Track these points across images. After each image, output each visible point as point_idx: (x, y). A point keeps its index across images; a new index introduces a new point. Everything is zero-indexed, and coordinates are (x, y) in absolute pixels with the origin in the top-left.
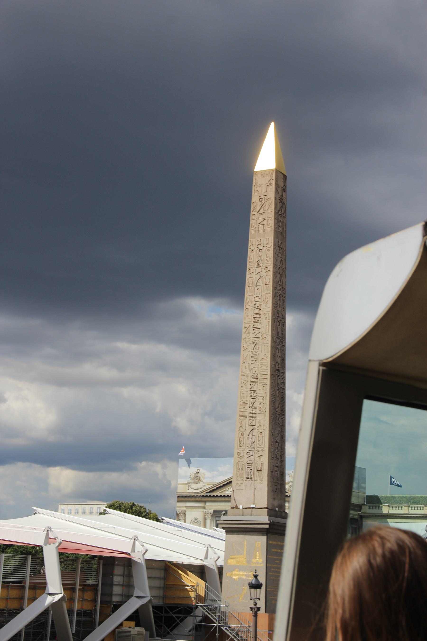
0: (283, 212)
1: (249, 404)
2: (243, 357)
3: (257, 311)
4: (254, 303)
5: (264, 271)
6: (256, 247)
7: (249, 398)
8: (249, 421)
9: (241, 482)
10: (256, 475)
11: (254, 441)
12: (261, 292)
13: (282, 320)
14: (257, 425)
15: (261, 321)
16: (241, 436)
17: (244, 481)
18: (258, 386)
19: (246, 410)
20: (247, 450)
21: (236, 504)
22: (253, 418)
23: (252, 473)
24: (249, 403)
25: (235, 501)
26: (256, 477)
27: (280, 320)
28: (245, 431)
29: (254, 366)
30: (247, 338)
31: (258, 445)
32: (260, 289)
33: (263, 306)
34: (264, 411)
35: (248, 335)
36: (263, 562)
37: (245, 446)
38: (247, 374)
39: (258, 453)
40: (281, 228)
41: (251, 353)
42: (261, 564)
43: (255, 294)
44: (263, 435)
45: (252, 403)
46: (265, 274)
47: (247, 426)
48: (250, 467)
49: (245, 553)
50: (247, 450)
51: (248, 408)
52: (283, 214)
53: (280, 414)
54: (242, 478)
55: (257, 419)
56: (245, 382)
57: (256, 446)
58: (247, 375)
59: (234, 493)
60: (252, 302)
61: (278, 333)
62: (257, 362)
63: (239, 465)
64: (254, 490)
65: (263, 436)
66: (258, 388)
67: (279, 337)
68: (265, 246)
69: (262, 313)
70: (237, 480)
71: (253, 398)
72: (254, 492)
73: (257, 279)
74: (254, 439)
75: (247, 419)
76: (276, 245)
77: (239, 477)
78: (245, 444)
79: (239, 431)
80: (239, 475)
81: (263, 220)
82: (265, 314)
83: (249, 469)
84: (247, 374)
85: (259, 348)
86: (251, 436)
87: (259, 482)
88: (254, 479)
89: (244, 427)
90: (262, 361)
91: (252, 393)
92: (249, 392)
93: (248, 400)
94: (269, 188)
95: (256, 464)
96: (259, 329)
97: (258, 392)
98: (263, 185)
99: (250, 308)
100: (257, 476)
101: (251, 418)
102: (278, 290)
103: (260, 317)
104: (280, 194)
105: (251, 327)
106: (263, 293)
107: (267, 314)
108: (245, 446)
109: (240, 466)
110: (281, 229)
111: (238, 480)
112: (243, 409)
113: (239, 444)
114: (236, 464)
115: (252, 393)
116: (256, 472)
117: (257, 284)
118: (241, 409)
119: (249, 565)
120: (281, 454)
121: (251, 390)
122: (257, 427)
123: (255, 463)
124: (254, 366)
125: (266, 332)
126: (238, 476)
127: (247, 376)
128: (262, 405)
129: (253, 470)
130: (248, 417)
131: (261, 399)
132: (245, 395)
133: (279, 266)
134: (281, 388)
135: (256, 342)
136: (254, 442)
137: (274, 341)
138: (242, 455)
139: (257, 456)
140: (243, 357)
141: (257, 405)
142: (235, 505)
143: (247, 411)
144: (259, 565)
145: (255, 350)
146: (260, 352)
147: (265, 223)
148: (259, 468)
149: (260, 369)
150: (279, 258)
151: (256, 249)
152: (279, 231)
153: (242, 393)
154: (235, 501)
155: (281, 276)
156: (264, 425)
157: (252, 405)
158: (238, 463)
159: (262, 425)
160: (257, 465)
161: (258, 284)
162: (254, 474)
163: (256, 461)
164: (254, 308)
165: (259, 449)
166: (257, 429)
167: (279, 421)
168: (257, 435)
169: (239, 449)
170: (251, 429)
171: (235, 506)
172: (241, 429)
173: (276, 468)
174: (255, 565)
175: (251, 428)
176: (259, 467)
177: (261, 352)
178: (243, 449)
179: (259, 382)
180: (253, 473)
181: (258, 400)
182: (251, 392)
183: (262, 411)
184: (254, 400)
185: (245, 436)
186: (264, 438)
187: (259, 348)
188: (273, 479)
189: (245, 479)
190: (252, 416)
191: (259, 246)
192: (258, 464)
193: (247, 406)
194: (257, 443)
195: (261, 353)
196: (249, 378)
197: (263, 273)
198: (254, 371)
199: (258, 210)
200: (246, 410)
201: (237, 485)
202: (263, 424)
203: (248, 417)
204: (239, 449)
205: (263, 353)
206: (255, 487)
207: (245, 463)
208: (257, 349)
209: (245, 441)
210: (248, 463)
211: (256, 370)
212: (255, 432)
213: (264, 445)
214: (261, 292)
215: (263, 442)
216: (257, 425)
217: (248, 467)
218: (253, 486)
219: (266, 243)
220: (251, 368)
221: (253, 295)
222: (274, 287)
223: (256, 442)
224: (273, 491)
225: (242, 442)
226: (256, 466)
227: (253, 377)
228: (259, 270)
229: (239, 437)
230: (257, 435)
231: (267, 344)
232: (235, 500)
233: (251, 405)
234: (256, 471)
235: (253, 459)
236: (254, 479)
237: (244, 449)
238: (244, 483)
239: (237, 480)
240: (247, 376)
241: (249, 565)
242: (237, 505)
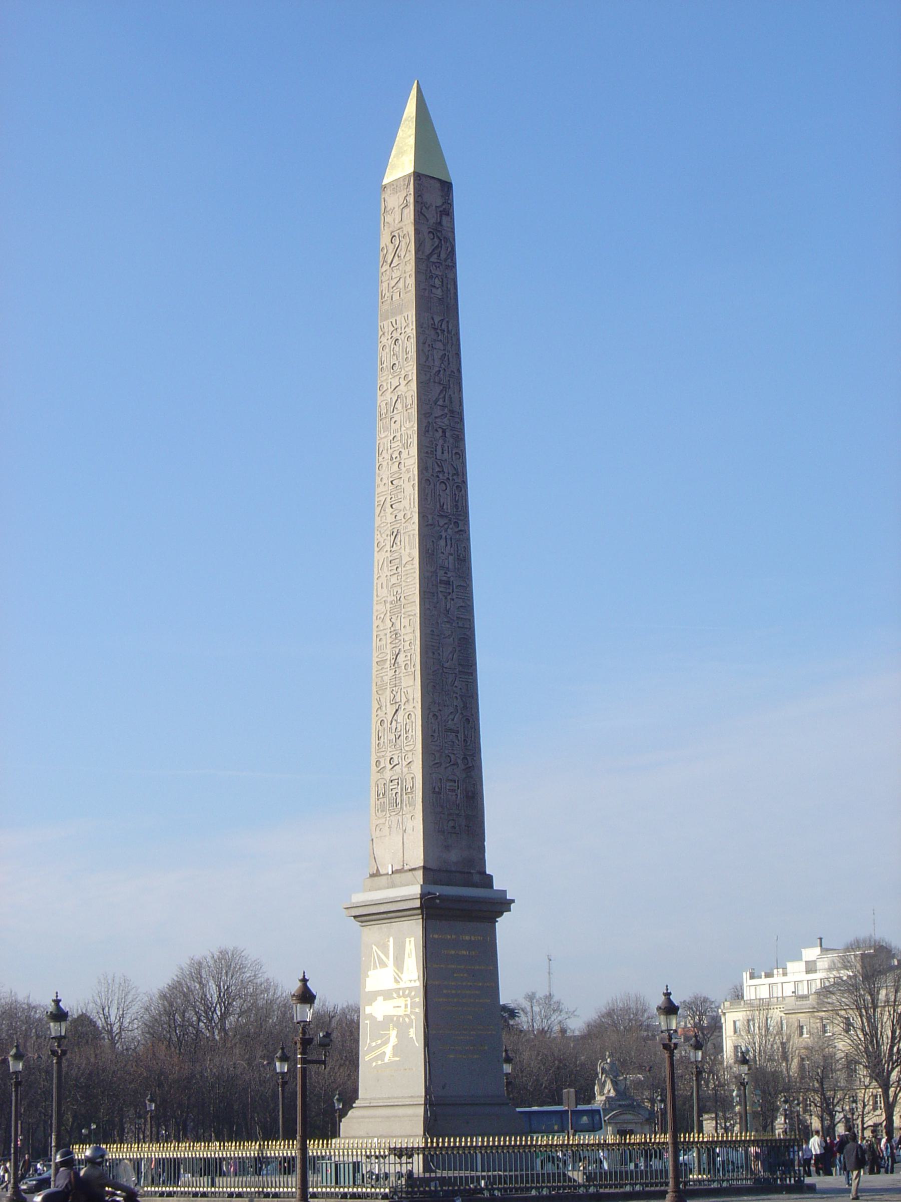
0: (443, 256)
4: (390, 451)
6: (390, 338)
8: (392, 695)
10: (404, 804)
11: (399, 734)
13: (455, 477)
14: (404, 700)
15: (402, 487)
17: (388, 819)
25: (375, 861)
27: (448, 479)
28: (386, 716)
29: (394, 580)
30: (382, 525)
32: (398, 423)
34: (413, 670)
40: (440, 289)
41: (388, 554)
43: (392, 433)
45: (395, 657)
47: (388, 704)
52: (446, 260)
53: (457, 671)
58: (385, 601)
61: (442, 507)
62: (399, 570)
67: (448, 514)
69: (404, 469)
71: (394, 646)
74: (399, 729)
75: (388, 691)
76: (425, 326)
81: (398, 279)
82: (408, 471)
87: (409, 816)
90: (407, 568)
92: (389, 635)
93: (389, 652)
94: (406, 211)
96: (401, 502)
98: (396, 209)
100: (406, 805)
101: (394, 688)
102: (436, 418)
103: (401, 478)
104: (432, 221)
105: (388, 499)
106: (403, 428)
109: (380, 789)
110: (439, 292)
112: (381, 672)
118: (378, 673)
120: (465, 754)
122: (402, 704)
124: (394, 580)
125: (410, 507)
132: (383, 642)
133: (437, 369)
134: (457, 618)
136: (400, 736)
137: (430, 522)
139: (405, 763)
141: (401, 658)
143: (387, 675)
149: (404, 584)
150: (435, 351)
151: (390, 341)
152: (432, 296)
154: (375, 861)
155: (445, 388)
159: (411, 699)
160: (406, 782)
165: (407, 748)
166: (402, 709)
167: (456, 687)
170: (395, 710)
173: (449, 784)
179: (403, 610)
181: (402, 650)
183: (409, 670)
188: (442, 807)
190: (394, 682)
193: (388, 664)
199: (389, 262)
204: (378, 754)
207: (388, 781)
209: (386, 737)
215: (414, 732)
219: (404, 324)
220: (390, 584)
222: (423, 412)
224: (441, 831)
226: (404, 784)
231: (412, 532)
233: (393, 662)
237: (385, 753)
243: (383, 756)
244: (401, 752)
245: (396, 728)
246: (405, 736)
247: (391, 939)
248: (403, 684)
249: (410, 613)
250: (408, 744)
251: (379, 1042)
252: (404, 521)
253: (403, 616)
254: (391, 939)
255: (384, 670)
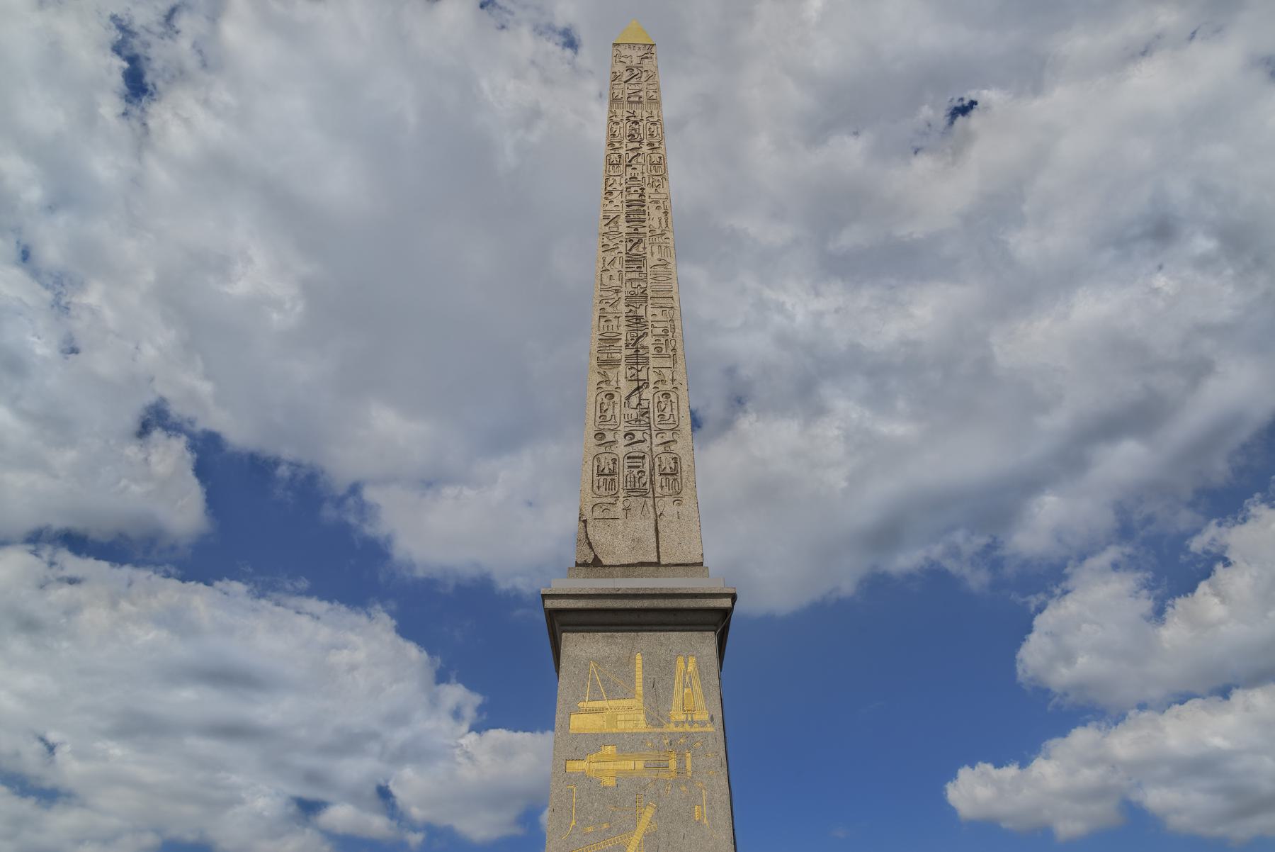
1: (627, 340)
2: (604, 261)
3: (636, 197)
4: (625, 186)
5: (645, 149)
7: (623, 330)
9: (612, 500)
10: (658, 485)
12: (643, 173)
14: (653, 378)
16: (605, 401)
17: (621, 499)
18: (649, 308)
19: (618, 351)
20: (628, 429)
21: (596, 556)
22: (640, 367)
23: (646, 479)
24: (623, 338)
25: (591, 547)
26: (658, 489)
31: (657, 419)
33: (648, 190)
34: (671, 353)
35: (615, 229)
36: (712, 718)
37: (618, 420)
38: (615, 288)
39: (660, 435)
42: (703, 724)
44: (673, 397)
45: (635, 339)
46: (650, 152)
48: (638, 467)
49: (639, 689)
50: (623, 429)
51: (623, 348)
54: (614, 492)
55: (651, 368)
56: (611, 302)
57: (654, 422)
59: (586, 526)
60: (621, 184)
63: (603, 461)
64: (656, 520)
65: (671, 401)
66: (649, 313)
68: (644, 118)
70: (595, 496)
72: (657, 523)
73: (631, 155)
74: (645, 404)
75: (622, 368)
77: (602, 489)
78: (618, 416)
79: (599, 391)
80: (601, 483)
83: (636, 471)
84: (615, 288)
85: (644, 248)
86: (634, 400)
88: (654, 493)
89: (613, 383)
91: (635, 321)
92: (623, 319)
95: (656, 460)
97: (651, 318)
99: (616, 194)
101: (635, 366)
105: (623, 216)
106: (646, 175)
107: (661, 201)
108: (618, 420)
111: (600, 496)
112: (608, 348)
113: (600, 417)
114: (591, 458)
115: (635, 321)
116: (658, 478)
117: (630, 161)
118: (601, 348)
119: (659, 730)
121: (631, 314)
123: (654, 457)
126: (598, 487)
127: (617, 291)
128: (663, 341)
129: (647, 473)
130: (623, 363)
131: (659, 331)
132: (615, 322)
135: (636, 240)
136: (647, 412)
138: (609, 437)
139: (657, 441)
140: (604, 261)
141: (648, 341)
142: (592, 556)
144: (696, 729)
145: (634, 251)
146: (648, 256)
147: (641, 94)
148: (668, 467)
149: (650, 281)
153: (603, 320)
154: (591, 547)
156: (673, 380)
157: (633, 342)
158: (600, 456)
161: (633, 162)
162: (651, 479)
163: (655, 454)
164: (625, 193)
165: (661, 427)
166: (651, 386)
168: (653, 398)
169: (601, 427)
171: (590, 561)
172: (603, 385)
174: (681, 730)
175: (635, 385)
176: (668, 465)
177: (652, 254)
178: (612, 427)
179: (650, 302)
180: (648, 480)
182: (630, 318)
184: (640, 333)
185: (616, 399)
186: (675, 406)
187: (644, 248)
189: (622, 494)
191: (633, 119)
192: (663, 459)
193: (622, 343)
194: (656, 416)
195: (652, 255)
196: (623, 295)
197: (645, 149)
198: (635, 284)
200: (618, 351)
201: (596, 508)
202: (671, 377)
203: (623, 363)
204: (601, 427)
205: (657, 256)
206: (658, 513)
208: (641, 249)
210: (629, 458)
211: (641, 283)
212: (647, 394)
213: (679, 419)
214: (643, 173)
215: (675, 413)
216: (653, 378)
217: (629, 467)
218: (651, 510)
221: (624, 174)
223: (652, 410)
225: (609, 413)
227: (633, 293)
228: (636, 145)
229: (599, 401)
230: (653, 398)
232: (590, 544)
234: (657, 474)
235: (647, 450)
236: (651, 492)
237: (616, 427)
238: (619, 504)
239: (595, 496)
240: (617, 291)
241: (659, 730)
242: (600, 556)
243: (612, 430)
244: (650, 429)
245: (639, 404)
246: (657, 414)
247: (638, 656)
248: (652, 363)
249: (663, 305)
250: (662, 422)
251: (605, 826)
252: (648, 234)
253: (650, 306)
254: (638, 656)
255: (613, 348)
